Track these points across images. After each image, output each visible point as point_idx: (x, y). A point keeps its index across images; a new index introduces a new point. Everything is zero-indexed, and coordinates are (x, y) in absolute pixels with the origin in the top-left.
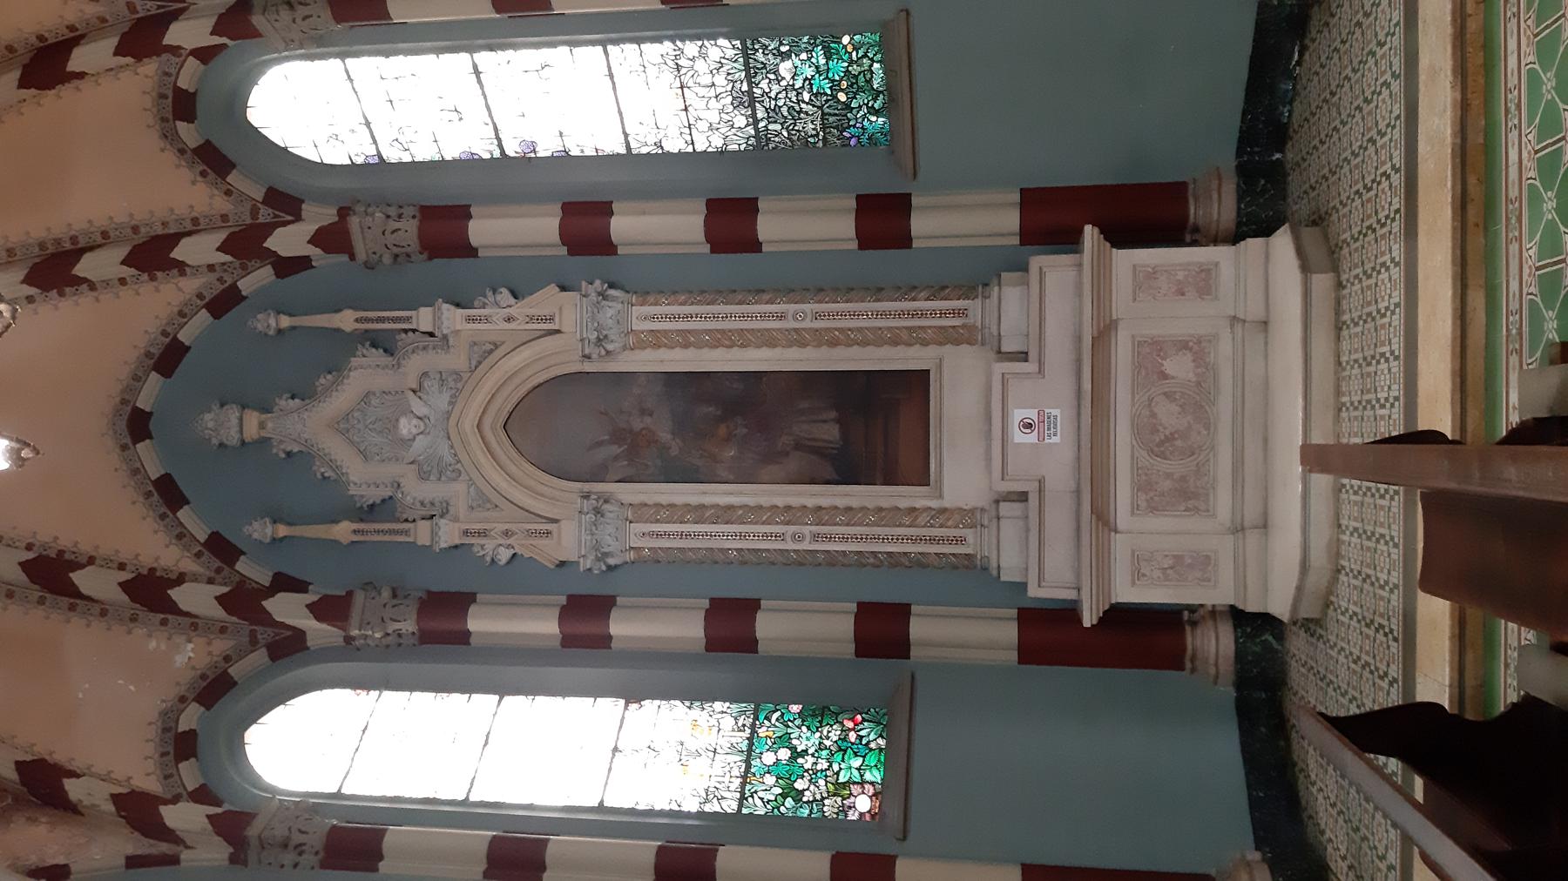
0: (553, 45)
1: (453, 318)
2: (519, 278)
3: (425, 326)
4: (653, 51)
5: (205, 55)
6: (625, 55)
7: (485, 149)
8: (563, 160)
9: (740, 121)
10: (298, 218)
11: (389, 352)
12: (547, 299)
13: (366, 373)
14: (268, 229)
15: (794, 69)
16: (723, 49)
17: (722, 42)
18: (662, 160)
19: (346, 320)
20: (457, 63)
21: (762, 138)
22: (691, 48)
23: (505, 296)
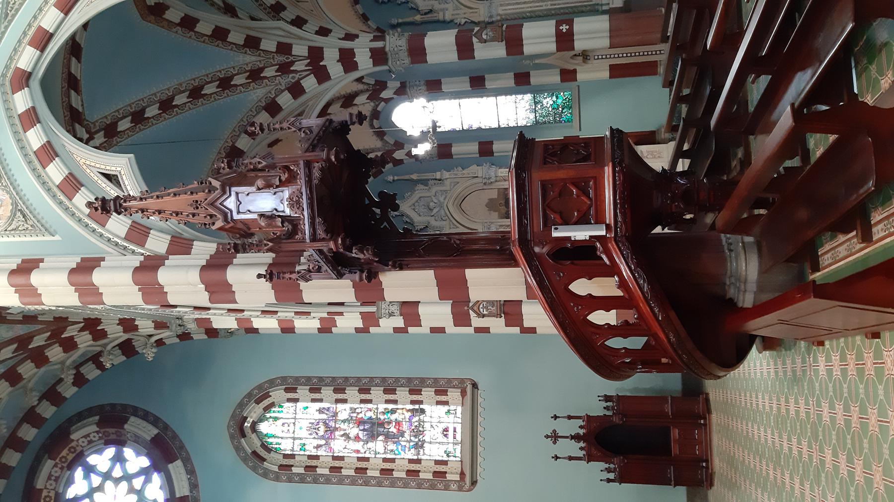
0: (482, 97)
1: (446, 175)
2: (465, 163)
3: (438, 177)
4: (511, 98)
5: (387, 101)
6: (502, 99)
7: (458, 127)
8: (480, 129)
9: (532, 116)
10: (402, 148)
11: (426, 185)
12: (474, 169)
13: (420, 191)
14: (393, 151)
15: (548, 101)
16: (528, 97)
17: (529, 95)
18: (509, 128)
19: (414, 177)
20: (454, 103)
21: (537, 122)
22: (520, 97)
23: (460, 169)
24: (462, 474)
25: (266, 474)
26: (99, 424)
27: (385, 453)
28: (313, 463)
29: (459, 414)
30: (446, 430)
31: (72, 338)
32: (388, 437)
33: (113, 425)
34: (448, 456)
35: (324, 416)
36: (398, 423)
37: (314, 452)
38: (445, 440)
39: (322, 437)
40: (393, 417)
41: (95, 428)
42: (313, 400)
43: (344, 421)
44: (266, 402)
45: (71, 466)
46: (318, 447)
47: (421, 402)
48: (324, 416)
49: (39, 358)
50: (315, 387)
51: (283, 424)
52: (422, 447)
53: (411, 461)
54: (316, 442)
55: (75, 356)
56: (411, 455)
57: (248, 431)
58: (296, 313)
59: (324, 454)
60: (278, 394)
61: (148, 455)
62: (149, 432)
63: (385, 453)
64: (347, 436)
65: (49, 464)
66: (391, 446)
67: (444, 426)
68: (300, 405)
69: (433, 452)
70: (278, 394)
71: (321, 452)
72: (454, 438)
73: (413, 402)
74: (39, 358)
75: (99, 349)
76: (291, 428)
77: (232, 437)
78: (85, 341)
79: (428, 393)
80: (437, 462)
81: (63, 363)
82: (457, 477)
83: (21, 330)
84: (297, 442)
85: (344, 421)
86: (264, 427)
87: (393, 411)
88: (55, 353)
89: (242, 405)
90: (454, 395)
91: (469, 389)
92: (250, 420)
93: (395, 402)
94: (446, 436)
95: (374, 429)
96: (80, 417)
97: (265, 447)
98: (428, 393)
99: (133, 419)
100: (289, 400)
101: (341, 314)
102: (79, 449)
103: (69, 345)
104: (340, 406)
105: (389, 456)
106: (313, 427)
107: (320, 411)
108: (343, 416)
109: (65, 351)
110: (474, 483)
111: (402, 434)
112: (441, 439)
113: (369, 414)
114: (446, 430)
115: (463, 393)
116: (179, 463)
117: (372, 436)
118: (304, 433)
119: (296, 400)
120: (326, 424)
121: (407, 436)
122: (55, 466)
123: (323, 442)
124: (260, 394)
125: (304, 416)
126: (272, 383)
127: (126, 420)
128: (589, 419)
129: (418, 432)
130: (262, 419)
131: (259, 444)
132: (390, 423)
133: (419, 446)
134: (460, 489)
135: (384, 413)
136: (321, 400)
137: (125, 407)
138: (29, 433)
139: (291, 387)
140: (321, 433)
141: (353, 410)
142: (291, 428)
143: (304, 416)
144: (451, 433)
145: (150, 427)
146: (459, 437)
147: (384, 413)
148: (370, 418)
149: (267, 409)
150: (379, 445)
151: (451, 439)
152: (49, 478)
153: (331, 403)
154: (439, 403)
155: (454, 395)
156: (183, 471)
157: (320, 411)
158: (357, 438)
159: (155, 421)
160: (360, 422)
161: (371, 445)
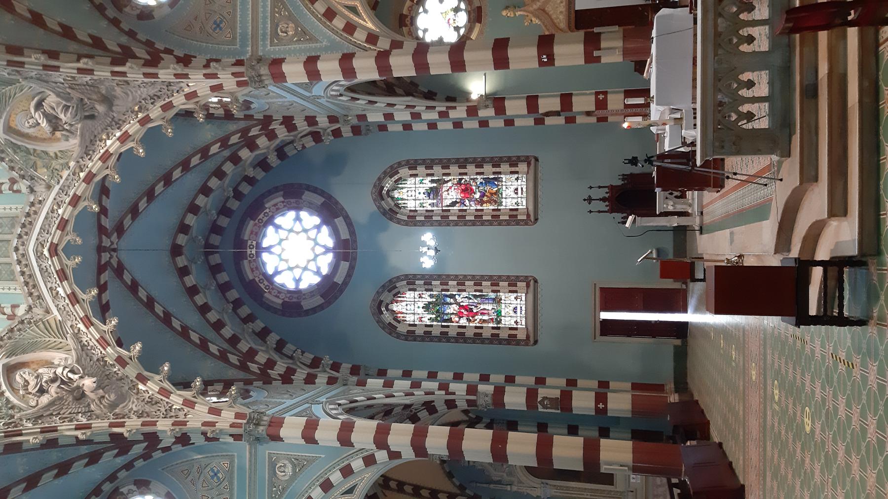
24: (528, 215)
25: (399, 222)
26: (284, 196)
28: (430, 214)
30: (517, 189)
31: (273, 130)
33: (294, 196)
37: (429, 208)
38: (515, 196)
41: (281, 199)
42: (428, 175)
44: (396, 177)
45: (266, 225)
47: (500, 173)
49: (251, 145)
50: (429, 164)
55: (276, 142)
57: (385, 196)
58: (428, 108)
60: (404, 172)
61: (319, 216)
62: (319, 200)
65: (252, 222)
68: (418, 179)
69: (508, 203)
73: (494, 173)
74: (251, 145)
75: (292, 138)
76: (413, 193)
77: (374, 200)
78: (282, 133)
80: (511, 210)
81: (268, 148)
82: (525, 217)
83: (242, 124)
84: (418, 202)
88: (262, 142)
91: (531, 161)
94: (517, 193)
96: (270, 193)
97: (397, 205)
99: (306, 193)
100: (411, 176)
101: (455, 108)
102: (270, 214)
103: (272, 135)
107: (432, 181)
109: (269, 140)
110: (536, 220)
114: (517, 189)
116: (341, 218)
119: (415, 176)
122: (255, 225)
124: (392, 171)
126: (400, 165)
127: (303, 194)
128: (612, 188)
136: (432, 175)
137: (300, 185)
138: (234, 205)
145: (319, 197)
151: (520, 195)
152: (252, 233)
155: (522, 167)
159: (322, 193)
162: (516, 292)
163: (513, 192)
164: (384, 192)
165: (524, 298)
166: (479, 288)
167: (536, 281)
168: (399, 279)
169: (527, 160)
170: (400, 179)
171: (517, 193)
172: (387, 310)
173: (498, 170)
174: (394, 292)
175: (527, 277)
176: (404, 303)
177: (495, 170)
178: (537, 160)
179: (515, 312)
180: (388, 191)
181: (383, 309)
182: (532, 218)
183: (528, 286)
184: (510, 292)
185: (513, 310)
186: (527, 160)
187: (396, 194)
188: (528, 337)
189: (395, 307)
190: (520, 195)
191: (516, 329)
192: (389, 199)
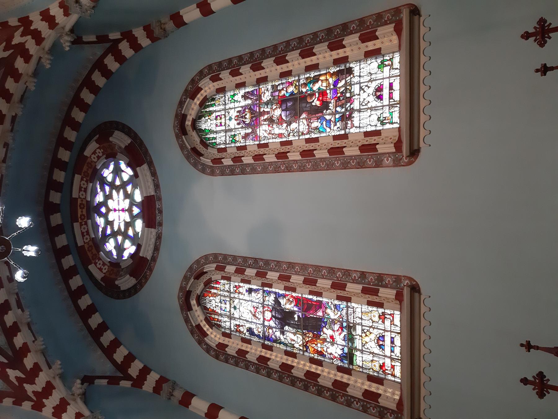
24: (398, 145)
25: (204, 169)
27: (308, 133)
29: (396, 64)
30: (380, 89)
32: (316, 112)
34: (383, 124)
35: (249, 102)
36: (323, 93)
38: (378, 104)
39: (248, 126)
40: (316, 87)
43: (267, 103)
44: (200, 97)
46: (246, 136)
48: (249, 102)
51: (216, 117)
52: (350, 117)
53: (336, 138)
54: (243, 132)
56: (335, 130)
59: (252, 143)
63: (308, 133)
64: (271, 121)
66: (316, 124)
67: (374, 85)
69: (364, 121)
70: (208, 87)
71: (249, 142)
72: (391, 97)
73: (337, 62)
79: (352, 44)
80: (367, 134)
84: (229, 134)
85: (267, 103)
86: (207, 124)
87: (316, 80)
89: (181, 104)
90: (387, 36)
92: (190, 118)
93: (315, 67)
95: (296, 105)
98: (352, 44)
104: (263, 87)
105: (313, 136)
106: (240, 116)
107: (245, 97)
108: (266, 97)
110: (414, 153)
111: (325, 105)
112: (374, 103)
113: (291, 89)
114: (380, 89)
115: (398, 31)
116: (145, 166)
117: (295, 116)
118: (233, 124)
120: (252, 111)
121: (331, 106)
123: (250, 131)
125: (232, 105)
129: (345, 99)
130: (200, 116)
131: (198, 140)
132: (312, 95)
133: (346, 118)
134: (397, 163)
135: (305, 85)
139: (213, 72)
140: (248, 121)
141: (275, 88)
142: (223, 121)
143: (232, 105)
144: (386, 93)
146: (396, 96)
147: (305, 85)
148: (292, 94)
149: (203, 104)
150: (302, 125)
153: (254, 86)
154: (369, 54)
155: (387, 36)
156: (148, 174)
157: (245, 97)
158: (280, 121)
160: (282, 102)
161: (294, 125)
162: (380, 305)
163: (374, 93)
164: (188, 123)
165: (397, 321)
166: (313, 288)
167: (415, 289)
168: (206, 259)
169: (393, 17)
170: (205, 99)
171: (380, 98)
172: (199, 304)
173: (341, 53)
174: (205, 278)
175: (398, 279)
176: (218, 299)
177: (336, 54)
178: (415, 11)
179: (381, 347)
180: (194, 123)
181: (193, 302)
182: (409, 146)
183: (399, 297)
184: (370, 303)
185: (373, 340)
186: (393, 17)
187: (207, 124)
188: (400, 403)
189: (213, 303)
190: (386, 101)
191: (379, 381)
192: (194, 134)
